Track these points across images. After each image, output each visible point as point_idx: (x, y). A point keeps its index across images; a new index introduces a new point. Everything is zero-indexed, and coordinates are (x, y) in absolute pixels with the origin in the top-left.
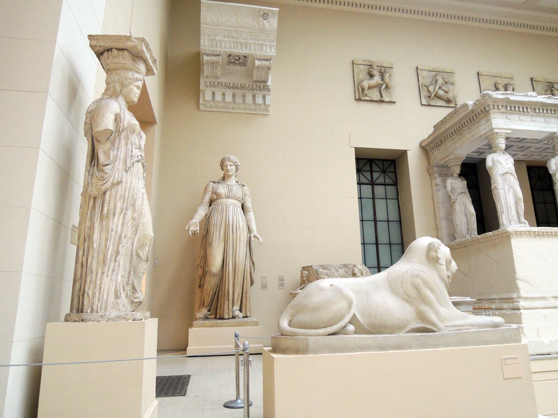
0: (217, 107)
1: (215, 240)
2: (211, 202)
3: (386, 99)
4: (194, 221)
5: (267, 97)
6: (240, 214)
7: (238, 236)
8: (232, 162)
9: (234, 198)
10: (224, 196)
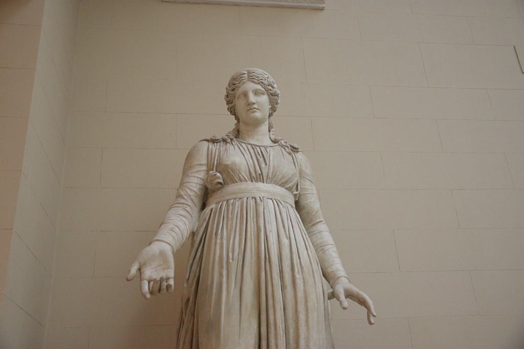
1: (228, 313)
2: (206, 195)
4: (156, 247)
7: (300, 294)
8: (261, 83)
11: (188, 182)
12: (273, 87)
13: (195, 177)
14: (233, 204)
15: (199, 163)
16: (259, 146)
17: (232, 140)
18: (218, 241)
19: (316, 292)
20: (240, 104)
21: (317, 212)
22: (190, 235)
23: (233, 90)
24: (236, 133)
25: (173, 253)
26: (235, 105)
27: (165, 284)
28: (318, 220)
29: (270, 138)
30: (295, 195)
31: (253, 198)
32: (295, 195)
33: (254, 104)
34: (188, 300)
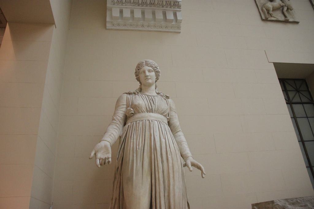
0: (125, 25)
2: (126, 119)
3: (291, 20)
4: (103, 144)
5: (178, 14)
6: (168, 133)
7: (170, 165)
8: (152, 67)
9: (157, 111)
10: (144, 109)
11: (118, 113)
12: (157, 69)
13: (121, 110)
14: (138, 123)
15: (123, 104)
16: (151, 96)
17: (138, 93)
18: (132, 141)
19: (178, 164)
20: (142, 76)
21: (178, 126)
22: (118, 138)
23: (139, 70)
24: (140, 90)
25: (111, 146)
26: (139, 77)
27: (107, 161)
28: (179, 130)
29: (156, 92)
30: (168, 119)
31: (148, 120)
32: (168, 119)
33: (148, 76)
34: (118, 168)
